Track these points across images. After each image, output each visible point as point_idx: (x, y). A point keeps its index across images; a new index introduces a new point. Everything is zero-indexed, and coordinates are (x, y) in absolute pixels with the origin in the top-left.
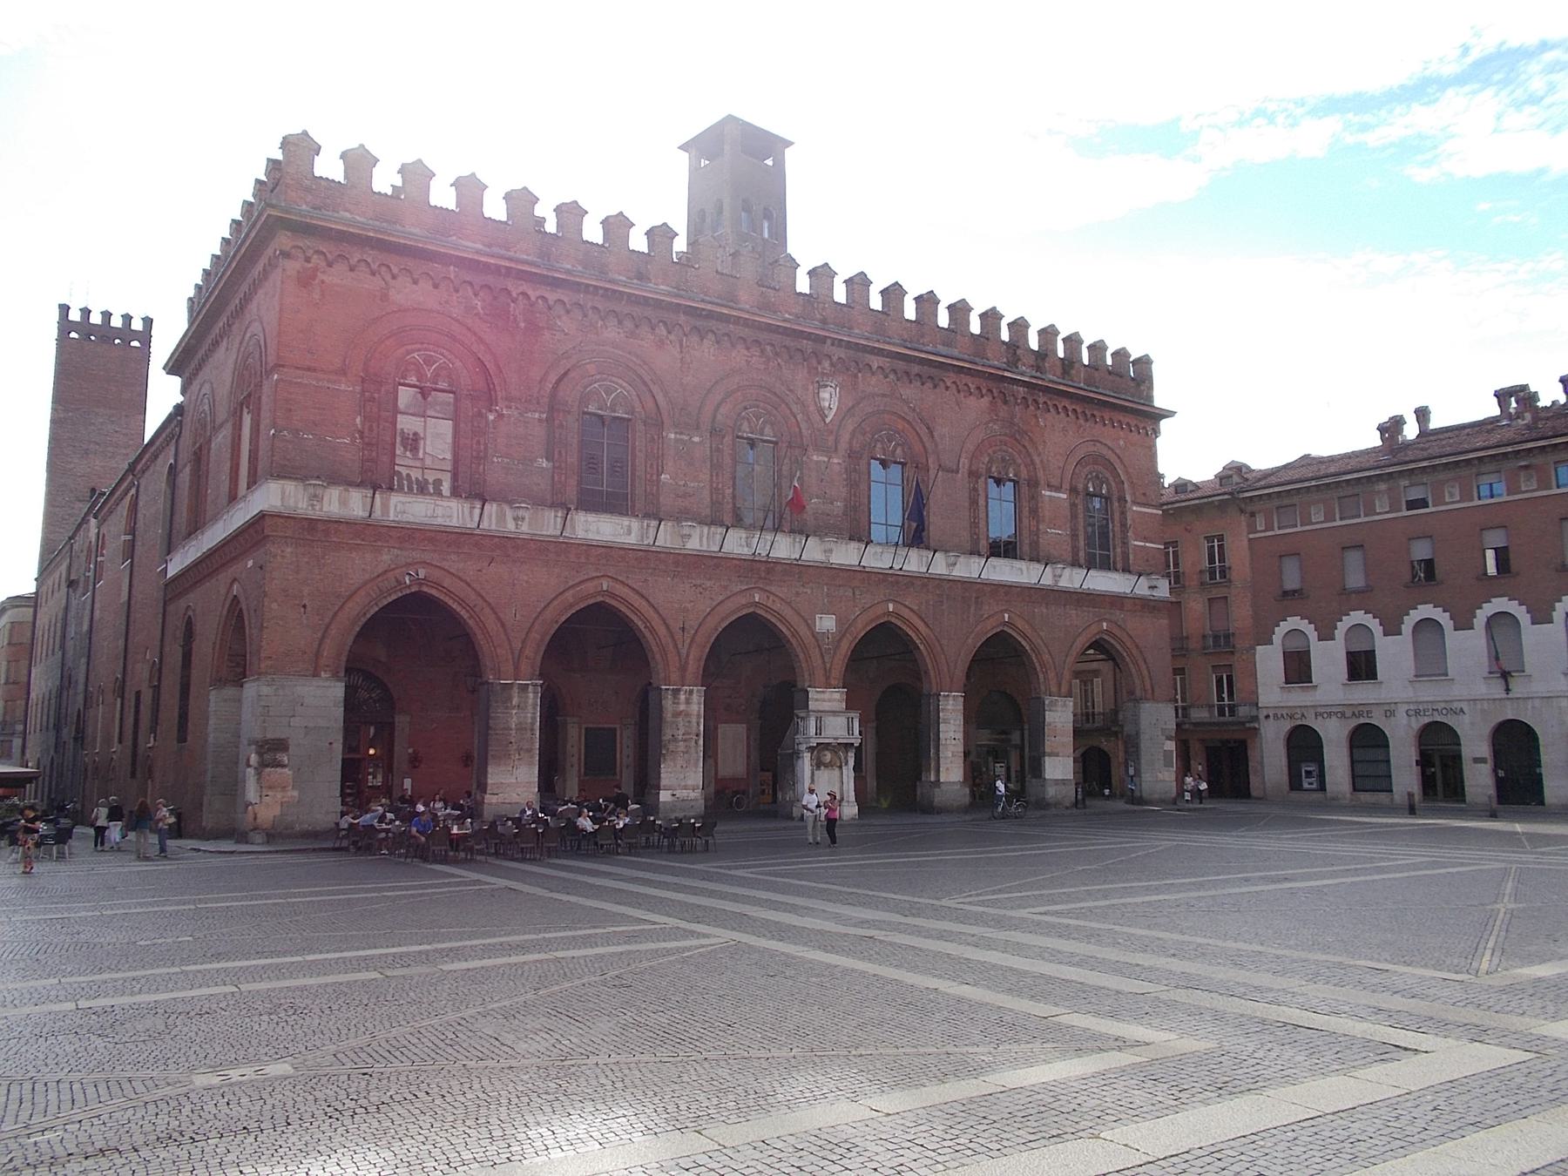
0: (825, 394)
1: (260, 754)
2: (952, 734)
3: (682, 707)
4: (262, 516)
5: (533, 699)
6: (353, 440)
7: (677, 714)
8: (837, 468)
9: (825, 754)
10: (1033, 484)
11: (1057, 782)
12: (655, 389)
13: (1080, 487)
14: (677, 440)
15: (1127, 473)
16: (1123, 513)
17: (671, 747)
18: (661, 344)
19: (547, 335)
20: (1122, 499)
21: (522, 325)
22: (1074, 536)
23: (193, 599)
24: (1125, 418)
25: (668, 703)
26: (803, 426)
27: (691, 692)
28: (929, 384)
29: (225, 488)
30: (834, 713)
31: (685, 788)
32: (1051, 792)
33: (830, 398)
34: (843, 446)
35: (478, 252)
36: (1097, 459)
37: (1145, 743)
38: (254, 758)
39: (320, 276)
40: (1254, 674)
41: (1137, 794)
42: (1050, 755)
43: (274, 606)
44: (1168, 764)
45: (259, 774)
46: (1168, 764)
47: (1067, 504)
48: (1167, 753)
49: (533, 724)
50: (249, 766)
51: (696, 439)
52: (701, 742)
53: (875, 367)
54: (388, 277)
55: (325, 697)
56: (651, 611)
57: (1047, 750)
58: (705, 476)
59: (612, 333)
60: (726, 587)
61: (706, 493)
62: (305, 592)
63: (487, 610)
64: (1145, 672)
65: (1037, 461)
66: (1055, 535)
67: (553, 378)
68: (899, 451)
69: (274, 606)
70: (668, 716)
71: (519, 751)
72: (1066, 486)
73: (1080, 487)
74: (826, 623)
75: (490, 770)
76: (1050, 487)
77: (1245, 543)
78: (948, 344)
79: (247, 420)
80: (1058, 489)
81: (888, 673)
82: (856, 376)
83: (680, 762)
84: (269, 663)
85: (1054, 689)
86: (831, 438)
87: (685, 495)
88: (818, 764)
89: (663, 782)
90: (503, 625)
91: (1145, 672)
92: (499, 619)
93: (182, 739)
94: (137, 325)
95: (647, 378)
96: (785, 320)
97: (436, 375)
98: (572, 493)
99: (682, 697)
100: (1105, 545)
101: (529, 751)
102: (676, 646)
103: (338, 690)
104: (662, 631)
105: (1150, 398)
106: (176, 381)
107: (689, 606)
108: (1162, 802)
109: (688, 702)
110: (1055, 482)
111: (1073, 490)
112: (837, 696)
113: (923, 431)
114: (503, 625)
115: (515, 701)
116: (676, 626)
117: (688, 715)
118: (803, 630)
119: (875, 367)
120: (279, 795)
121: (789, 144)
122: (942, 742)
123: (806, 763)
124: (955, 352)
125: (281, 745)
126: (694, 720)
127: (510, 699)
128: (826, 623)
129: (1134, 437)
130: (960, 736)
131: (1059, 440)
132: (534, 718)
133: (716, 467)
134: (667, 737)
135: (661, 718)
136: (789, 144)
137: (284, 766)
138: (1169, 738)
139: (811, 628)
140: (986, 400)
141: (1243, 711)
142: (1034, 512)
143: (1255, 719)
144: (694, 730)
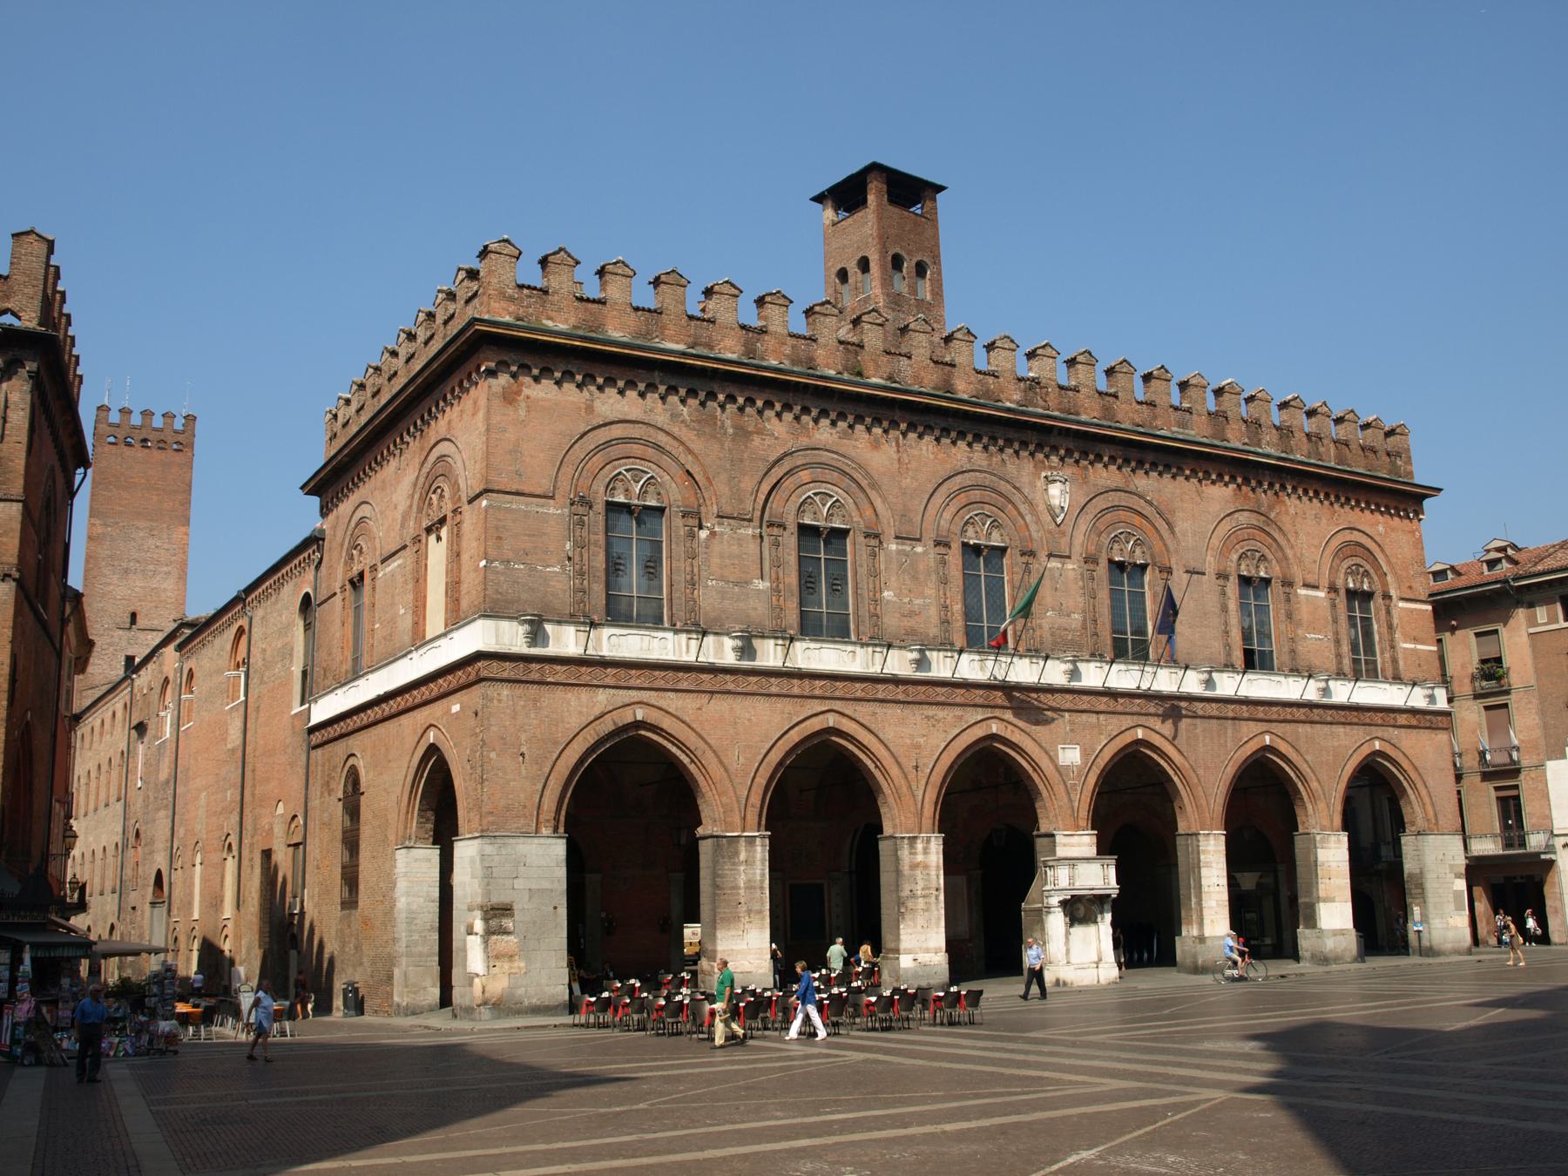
0: (1055, 490)
1: (486, 920)
2: (1215, 880)
3: (920, 858)
4: (479, 656)
5: (761, 852)
6: (563, 567)
7: (914, 866)
8: (1071, 575)
9: (1079, 909)
10: (1288, 583)
12: (873, 494)
14: (899, 552)
15: (1389, 563)
16: (1388, 612)
17: (910, 904)
18: (876, 445)
19: (757, 440)
20: (1386, 596)
21: (730, 431)
22: (1337, 642)
23: (363, 748)
25: (904, 853)
26: (1033, 528)
27: (928, 840)
29: (406, 623)
30: (1087, 859)
31: (927, 951)
34: (1077, 549)
35: (684, 354)
37: (1431, 885)
38: (479, 926)
39: (526, 391)
40: (1546, 796)
41: (1425, 943)
43: (493, 755)
44: (1459, 908)
45: (486, 942)
46: (1459, 908)
47: (1326, 604)
48: (1457, 894)
49: (762, 881)
50: (470, 932)
51: (919, 549)
52: (942, 897)
54: (593, 388)
55: (545, 859)
56: (882, 748)
57: (1322, 894)
58: (930, 591)
59: (825, 433)
60: (961, 718)
61: (933, 613)
62: (523, 737)
63: (709, 754)
64: (1427, 800)
65: (1289, 552)
66: (1316, 641)
67: (765, 488)
68: (1138, 551)
69: (493, 755)
70: (906, 869)
71: (749, 912)
72: (1325, 582)
73: (1340, 583)
74: (1071, 756)
75: (719, 934)
76: (1306, 585)
77: (1525, 638)
78: (1183, 425)
79: (437, 552)
80: (1315, 587)
81: (1135, 810)
82: (1086, 468)
83: (920, 920)
84: (491, 819)
86: (1064, 541)
87: (911, 614)
89: (903, 946)
90: (726, 770)
91: (1427, 800)
92: (721, 762)
93: (350, 903)
94: (179, 424)
95: (864, 483)
96: (1009, 410)
97: (643, 493)
98: (792, 617)
99: (919, 846)
100: (1370, 649)
101: (760, 912)
102: (910, 787)
103: (559, 848)
104: (894, 771)
105: (1411, 474)
106: (316, 500)
107: (922, 740)
108: (1457, 952)
109: (926, 851)
110: (1311, 579)
111: (1333, 589)
112: (1087, 839)
114: (726, 770)
115: (743, 856)
116: (909, 765)
117: (926, 867)
118: (1045, 763)
120: (506, 966)
121: (940, 189)
122: (1205, 889)
123: (1056, 921)
124: (1192, 434)
125: (506, 910)
126: (933, 873)
127: (737, 853)
128: (1071, 756)
130: (1224, 881)
131: (1311, 530)
132: (763, 875)
133: (944, 581)
134: (906, 893)
135: (898, 872)
136: (940, 189)
137: (509, 933)
138: (1458, 876)
139: (1054, 760)
140: (1232, 486)
141: (1535, 841)
142: (1289, 616)
143: (1550, 849)
144: (934, 884)
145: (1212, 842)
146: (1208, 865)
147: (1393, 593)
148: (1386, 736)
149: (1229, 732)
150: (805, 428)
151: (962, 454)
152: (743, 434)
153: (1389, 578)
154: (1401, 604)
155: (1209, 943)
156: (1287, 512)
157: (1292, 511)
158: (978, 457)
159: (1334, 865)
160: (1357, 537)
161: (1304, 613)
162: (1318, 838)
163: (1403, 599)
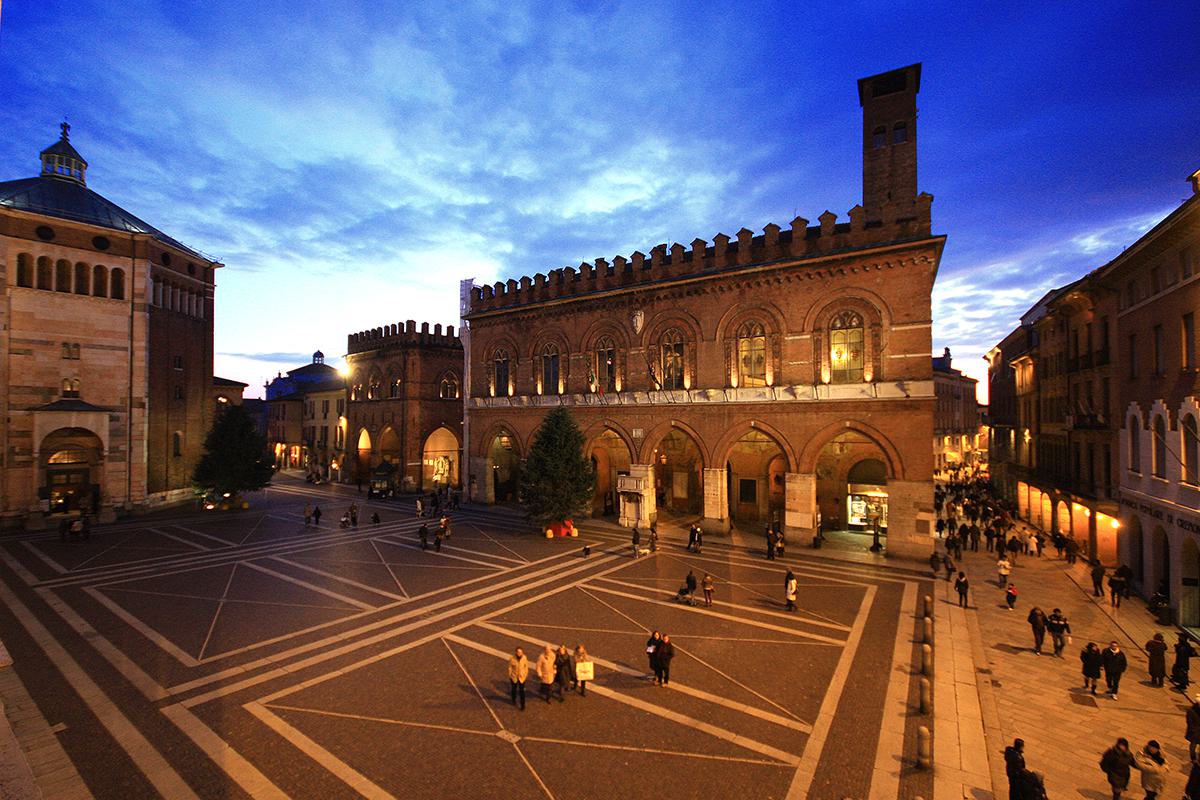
2: (712, 492)
11: (795, 529)
13: (824, 325)
19: (532, 331)
24: (876, 261)
28: (695, 296)
32: (789, 534)
33: (639, 322)
36: (844, 302)
42: (790, 510)
53: (662, 296)
57: (787, 507)
73: (824, 325)
76: (792, 333)
80: (803, 331)
85: (793, 467)
88: (630, 501)
111: (817, 330)
112: (644, 469)
113: (691, 321)
118: (627, 438)
119: (662, 296)
129: (898, 270)
145: (711, 473)
146: (709, 484)
147: (885, 322)
148: (858, 418)
149: (726, 420)
150: (545, 322)
151: (597, 314)
152: (528, 329)
153: (883, 314)
154: (894, 329)
155: (706, 520)
156: (780, 295)
157: (785, 291)
158: (605, 313)
159: (798, 492)
160: (849, 293)
161: (789, 350)
162: (787, 476)
163: (892, 324)
